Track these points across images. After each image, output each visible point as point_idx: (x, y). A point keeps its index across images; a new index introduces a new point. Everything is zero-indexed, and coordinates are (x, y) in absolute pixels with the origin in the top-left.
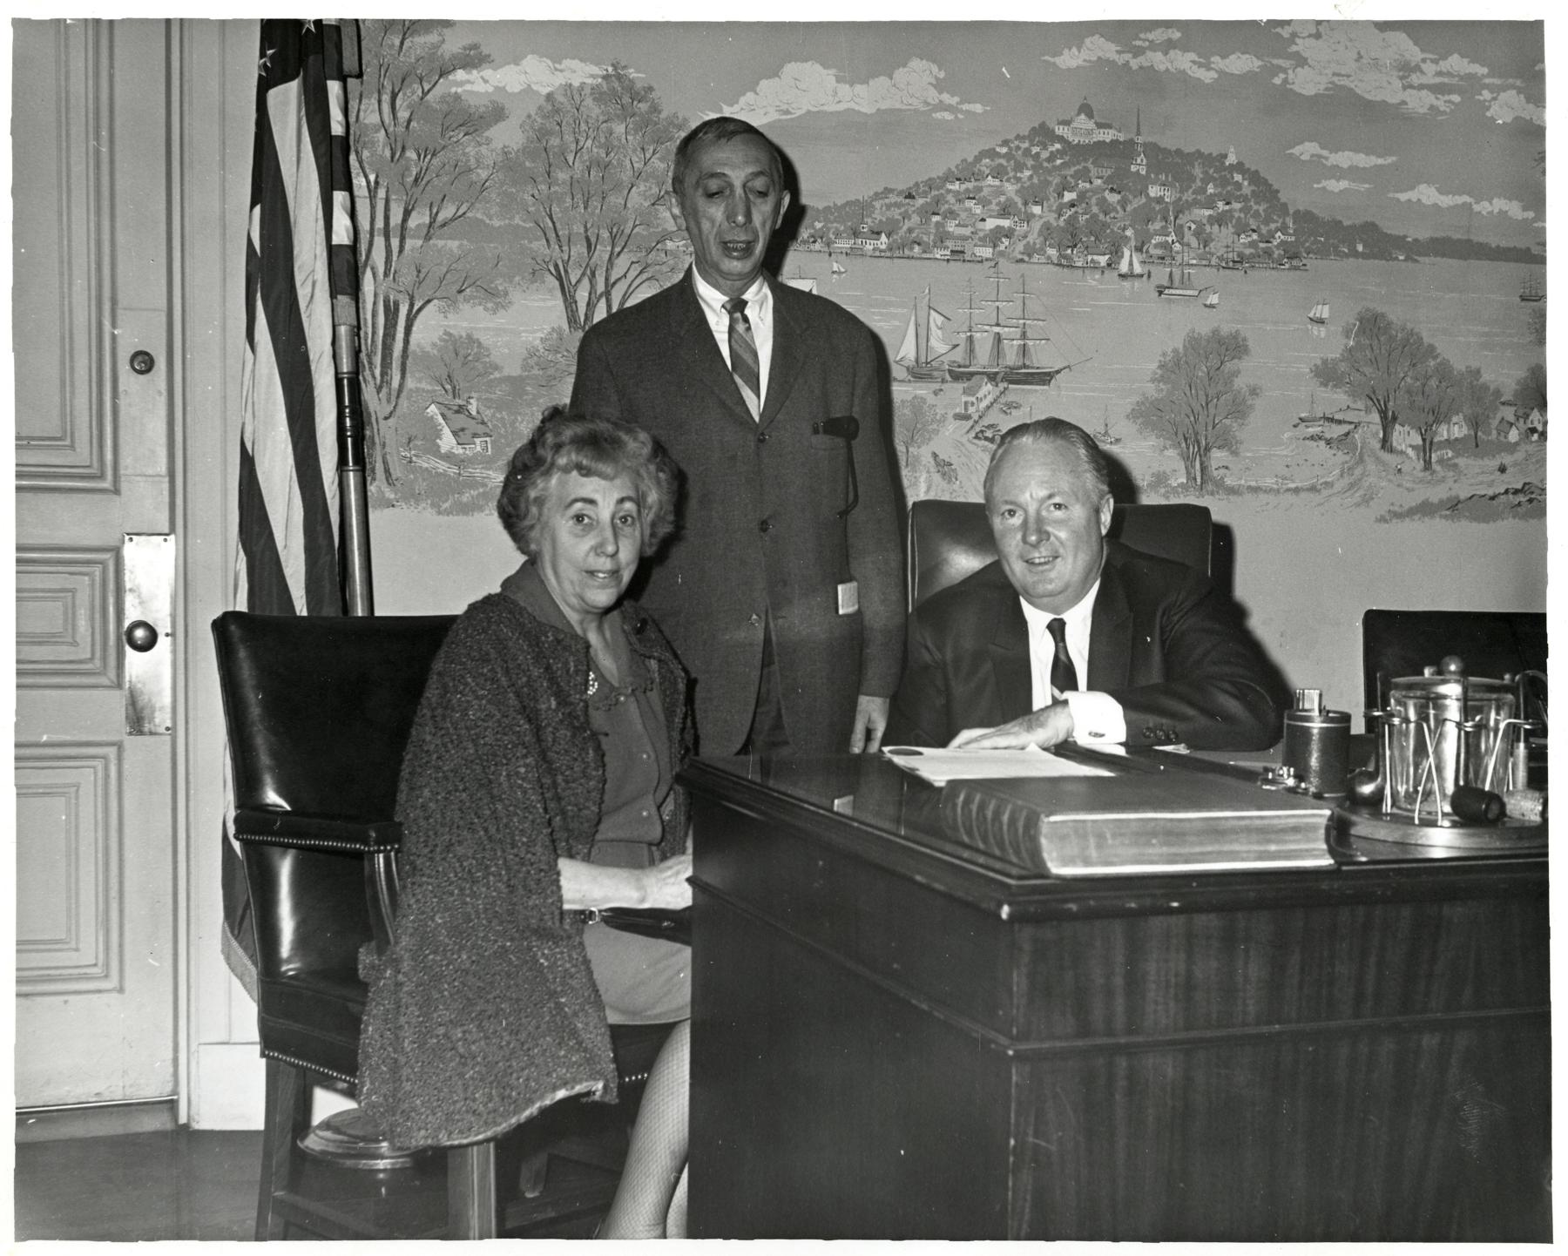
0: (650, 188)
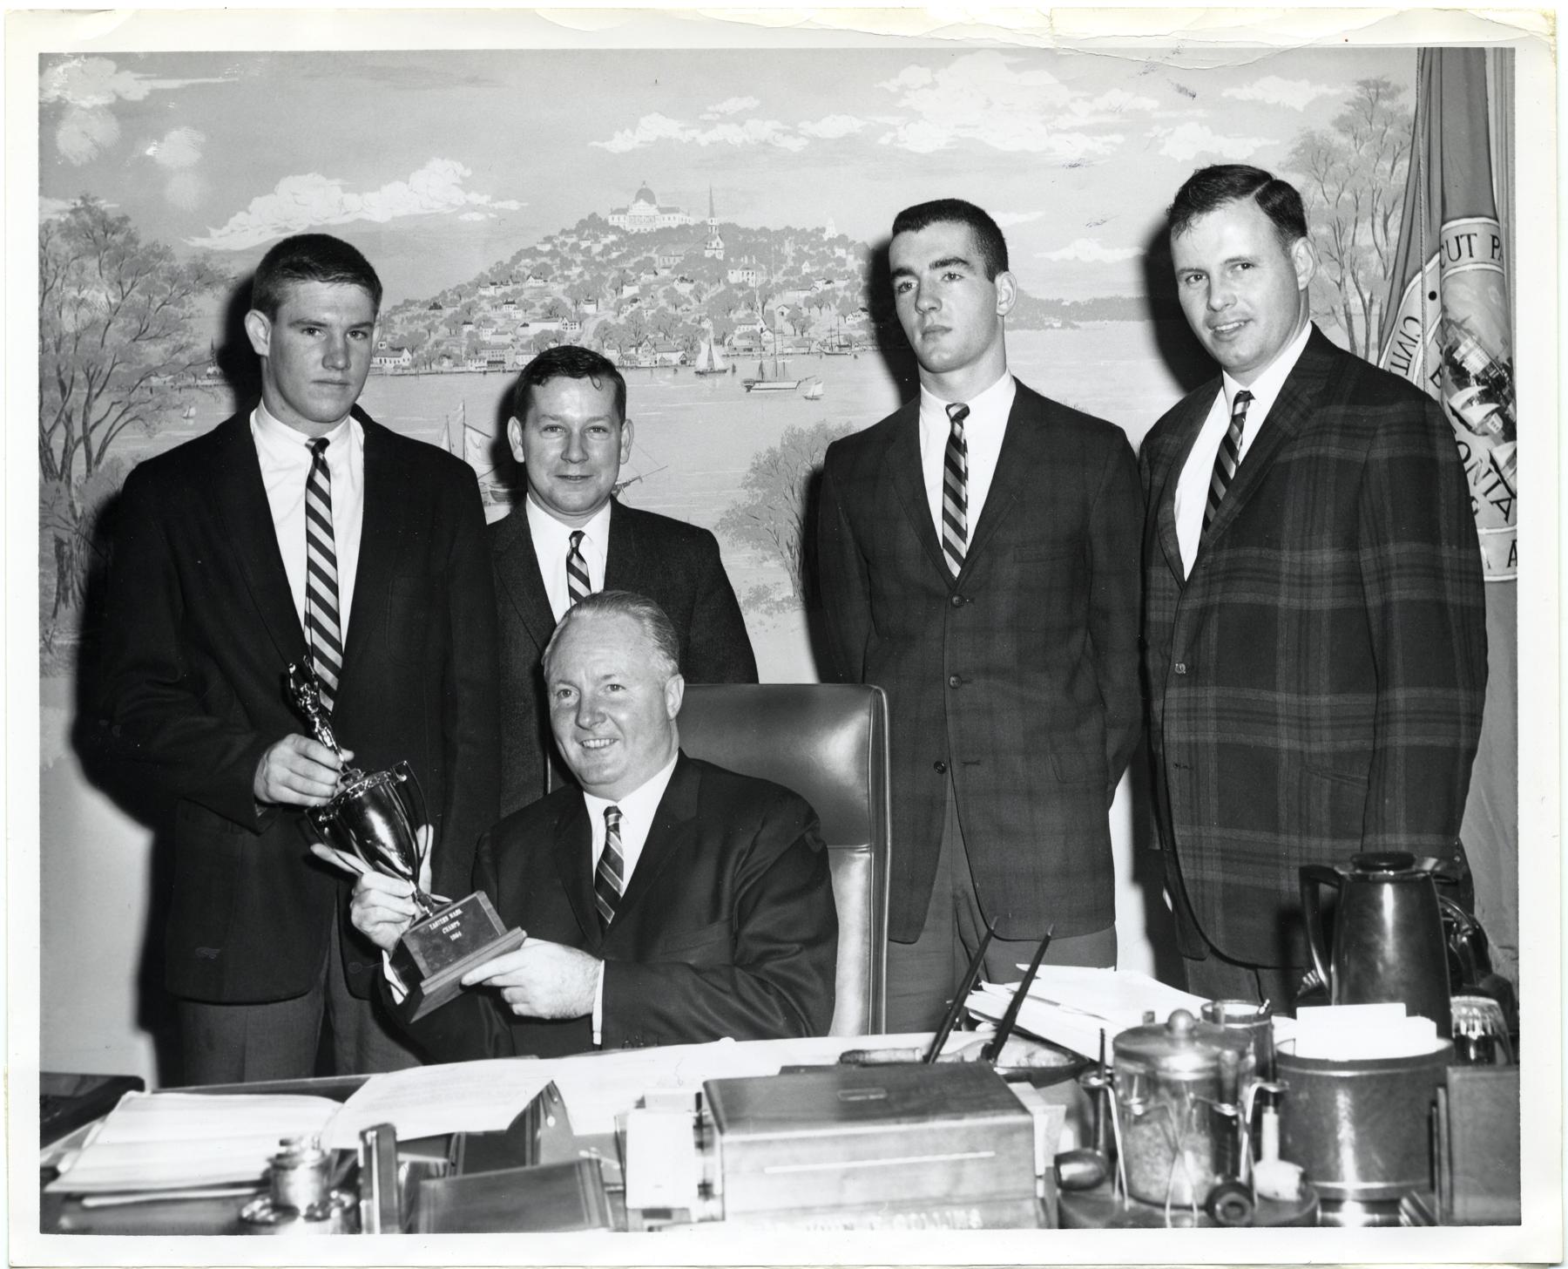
0: (130, 323)
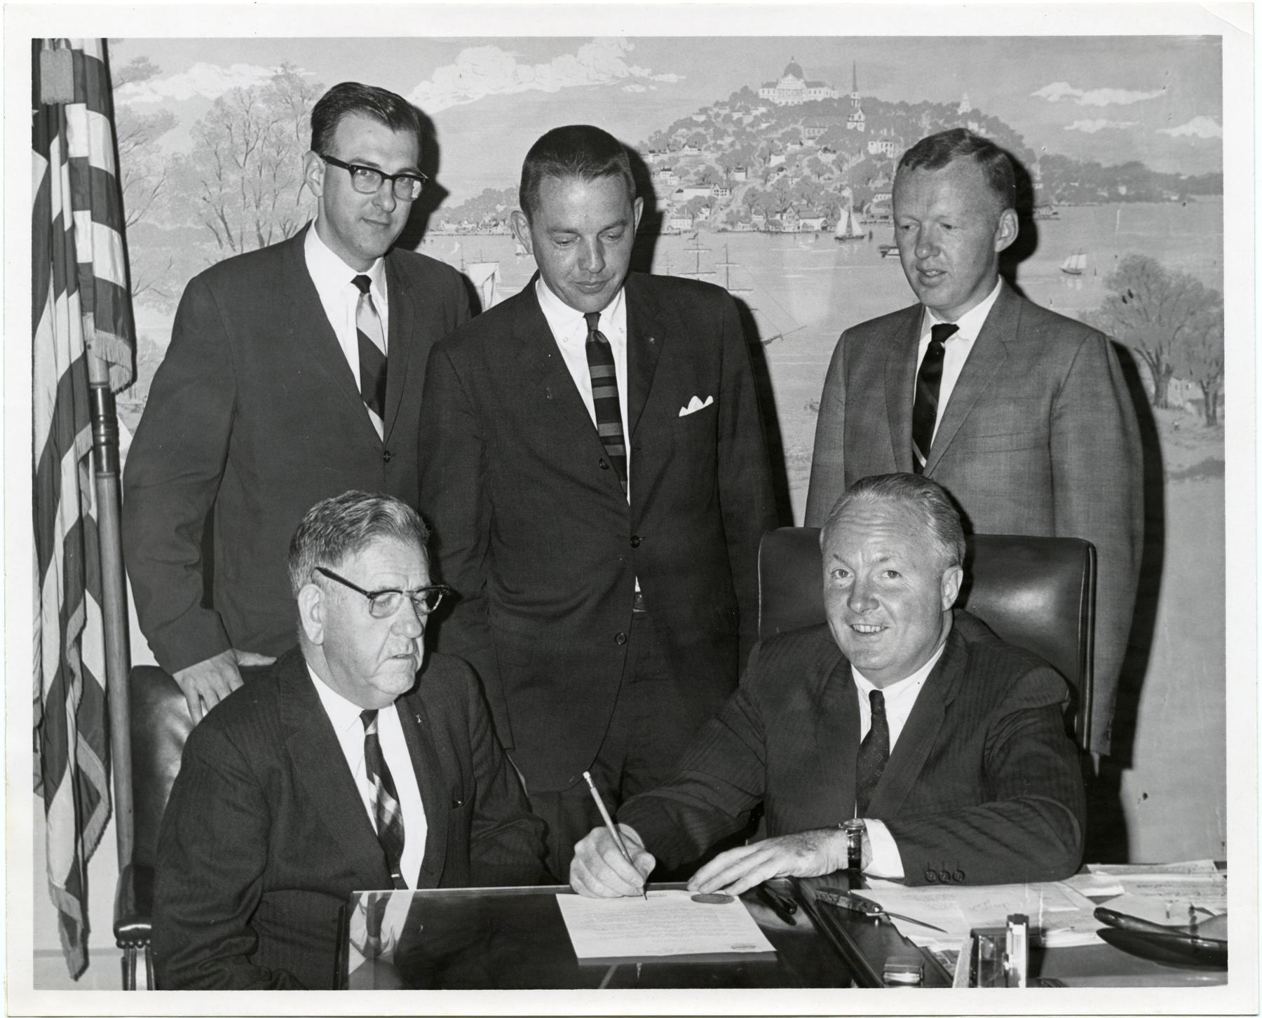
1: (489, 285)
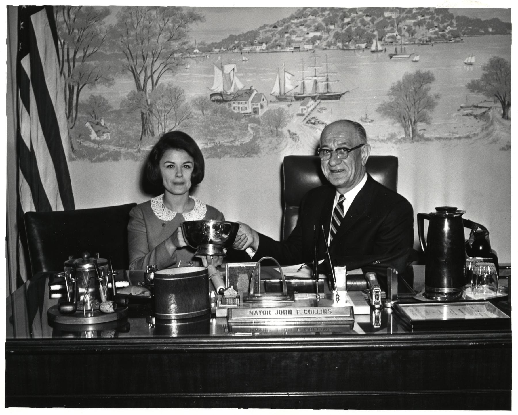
0: (167, 34)
1: (232, 73)
